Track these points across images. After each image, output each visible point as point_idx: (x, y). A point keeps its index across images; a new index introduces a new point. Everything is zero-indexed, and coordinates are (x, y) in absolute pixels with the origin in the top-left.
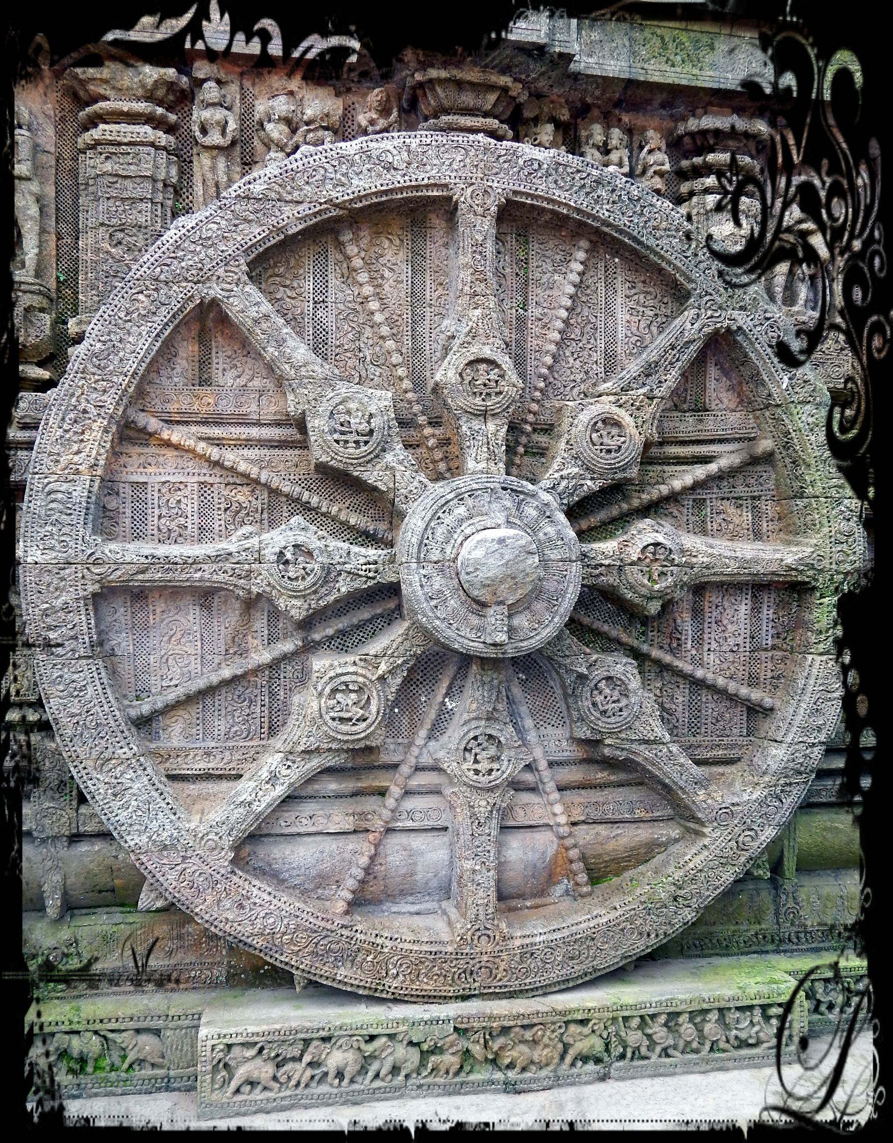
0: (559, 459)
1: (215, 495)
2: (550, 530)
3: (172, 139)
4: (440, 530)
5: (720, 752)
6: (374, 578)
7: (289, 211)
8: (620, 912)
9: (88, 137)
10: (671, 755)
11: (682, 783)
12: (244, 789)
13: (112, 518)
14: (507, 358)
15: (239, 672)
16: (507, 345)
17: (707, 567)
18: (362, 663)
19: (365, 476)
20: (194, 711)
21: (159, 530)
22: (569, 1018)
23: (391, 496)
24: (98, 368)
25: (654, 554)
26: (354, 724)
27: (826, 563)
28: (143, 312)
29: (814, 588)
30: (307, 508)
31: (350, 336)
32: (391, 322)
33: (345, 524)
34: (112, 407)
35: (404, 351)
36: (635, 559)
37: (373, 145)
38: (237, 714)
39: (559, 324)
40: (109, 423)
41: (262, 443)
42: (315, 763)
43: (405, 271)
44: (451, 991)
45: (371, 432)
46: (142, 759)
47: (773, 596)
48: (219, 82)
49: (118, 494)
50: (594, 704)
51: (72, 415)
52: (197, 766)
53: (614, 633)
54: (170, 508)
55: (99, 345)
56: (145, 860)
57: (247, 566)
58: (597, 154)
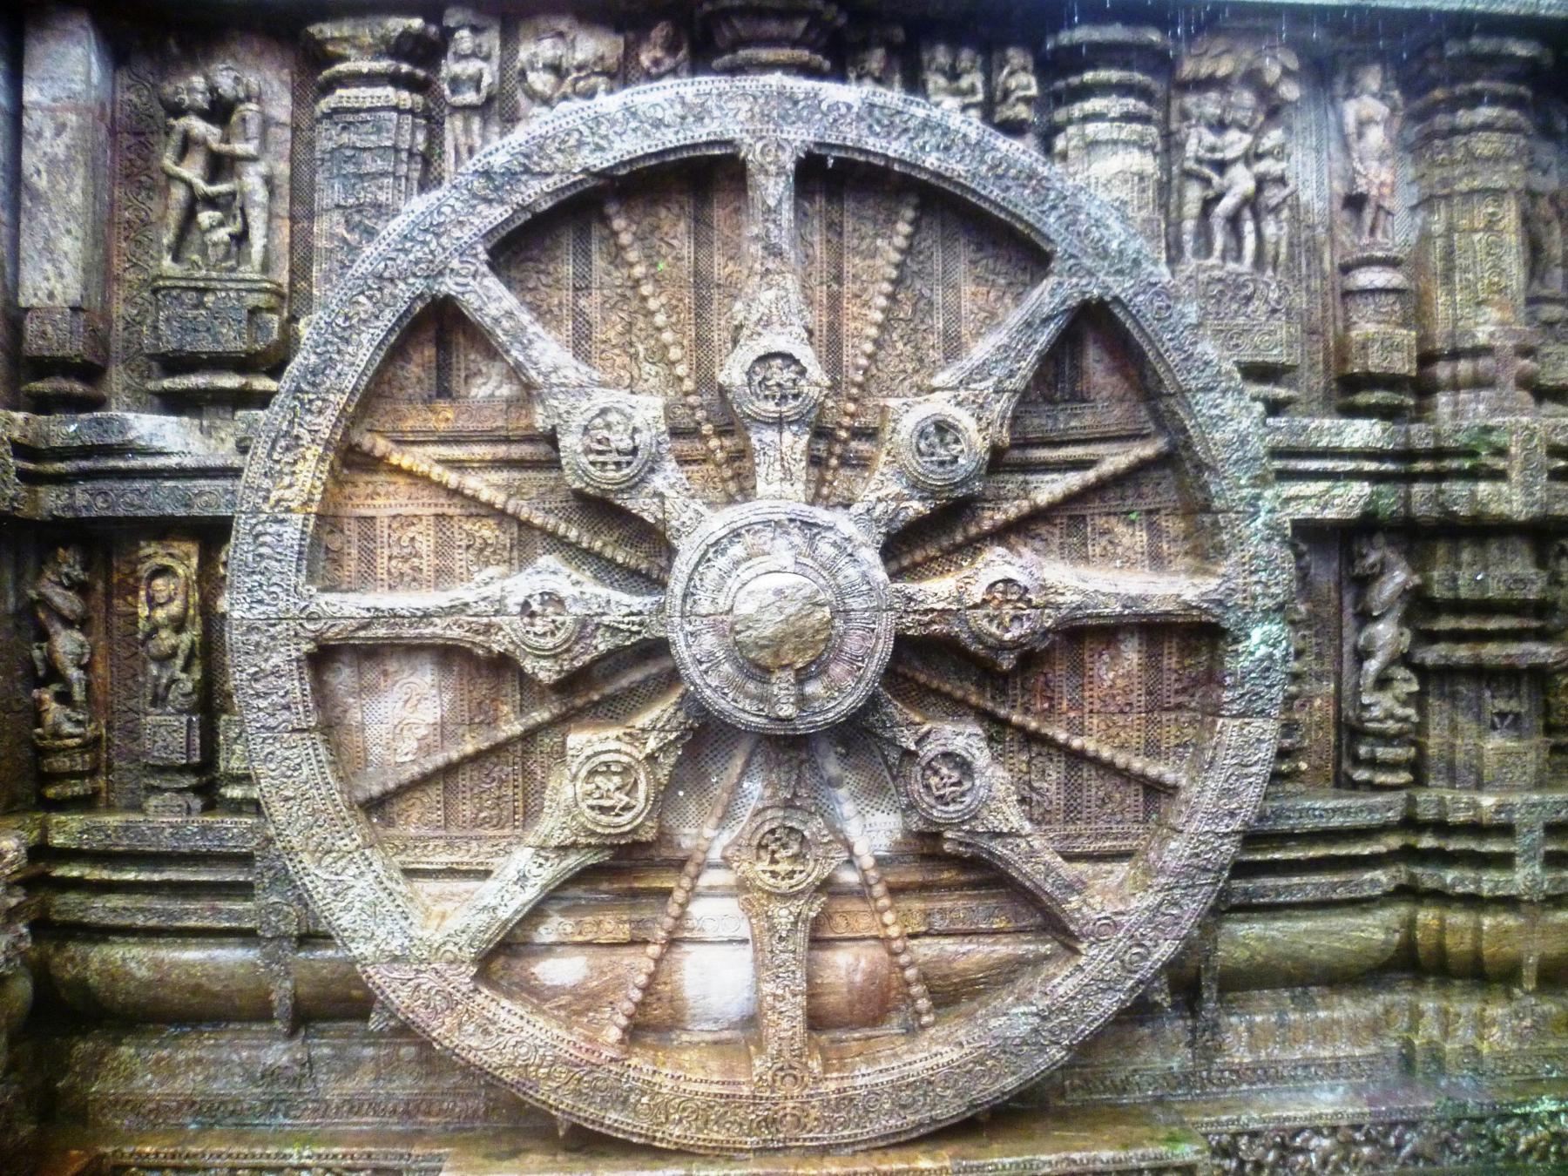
0: (877, 475)
2: (852, 572)
3: (419, 98)
5: (1108, 844)
6: (639, 633)
8: (967, 1049)
9: (325, 104)
10: (1032, 853)
12: (486, 891)
13: (335, 561)
14: (809, 351)
15: (485, 745)
16: (811, 333)
17: (1079, 608)
18: (627, 739)
19: (630, 505)
20: (435, 793)
21: (389, 572)
25: (1004, 593)
26: (617, 815)
28: (363, 316)
32: (671, 309)
33: (612, 561)
34: (328, 431)
35: (686, 342)
36: (978, 600)
37: (638, 99)
38: (485, 796)
39: (882, 302)
40: (326, 449)
42: (573, 861)
46: (368, 852)
49: (342, 531)
50: (927, 787)
51: (283, 443)
57: (485, 620)
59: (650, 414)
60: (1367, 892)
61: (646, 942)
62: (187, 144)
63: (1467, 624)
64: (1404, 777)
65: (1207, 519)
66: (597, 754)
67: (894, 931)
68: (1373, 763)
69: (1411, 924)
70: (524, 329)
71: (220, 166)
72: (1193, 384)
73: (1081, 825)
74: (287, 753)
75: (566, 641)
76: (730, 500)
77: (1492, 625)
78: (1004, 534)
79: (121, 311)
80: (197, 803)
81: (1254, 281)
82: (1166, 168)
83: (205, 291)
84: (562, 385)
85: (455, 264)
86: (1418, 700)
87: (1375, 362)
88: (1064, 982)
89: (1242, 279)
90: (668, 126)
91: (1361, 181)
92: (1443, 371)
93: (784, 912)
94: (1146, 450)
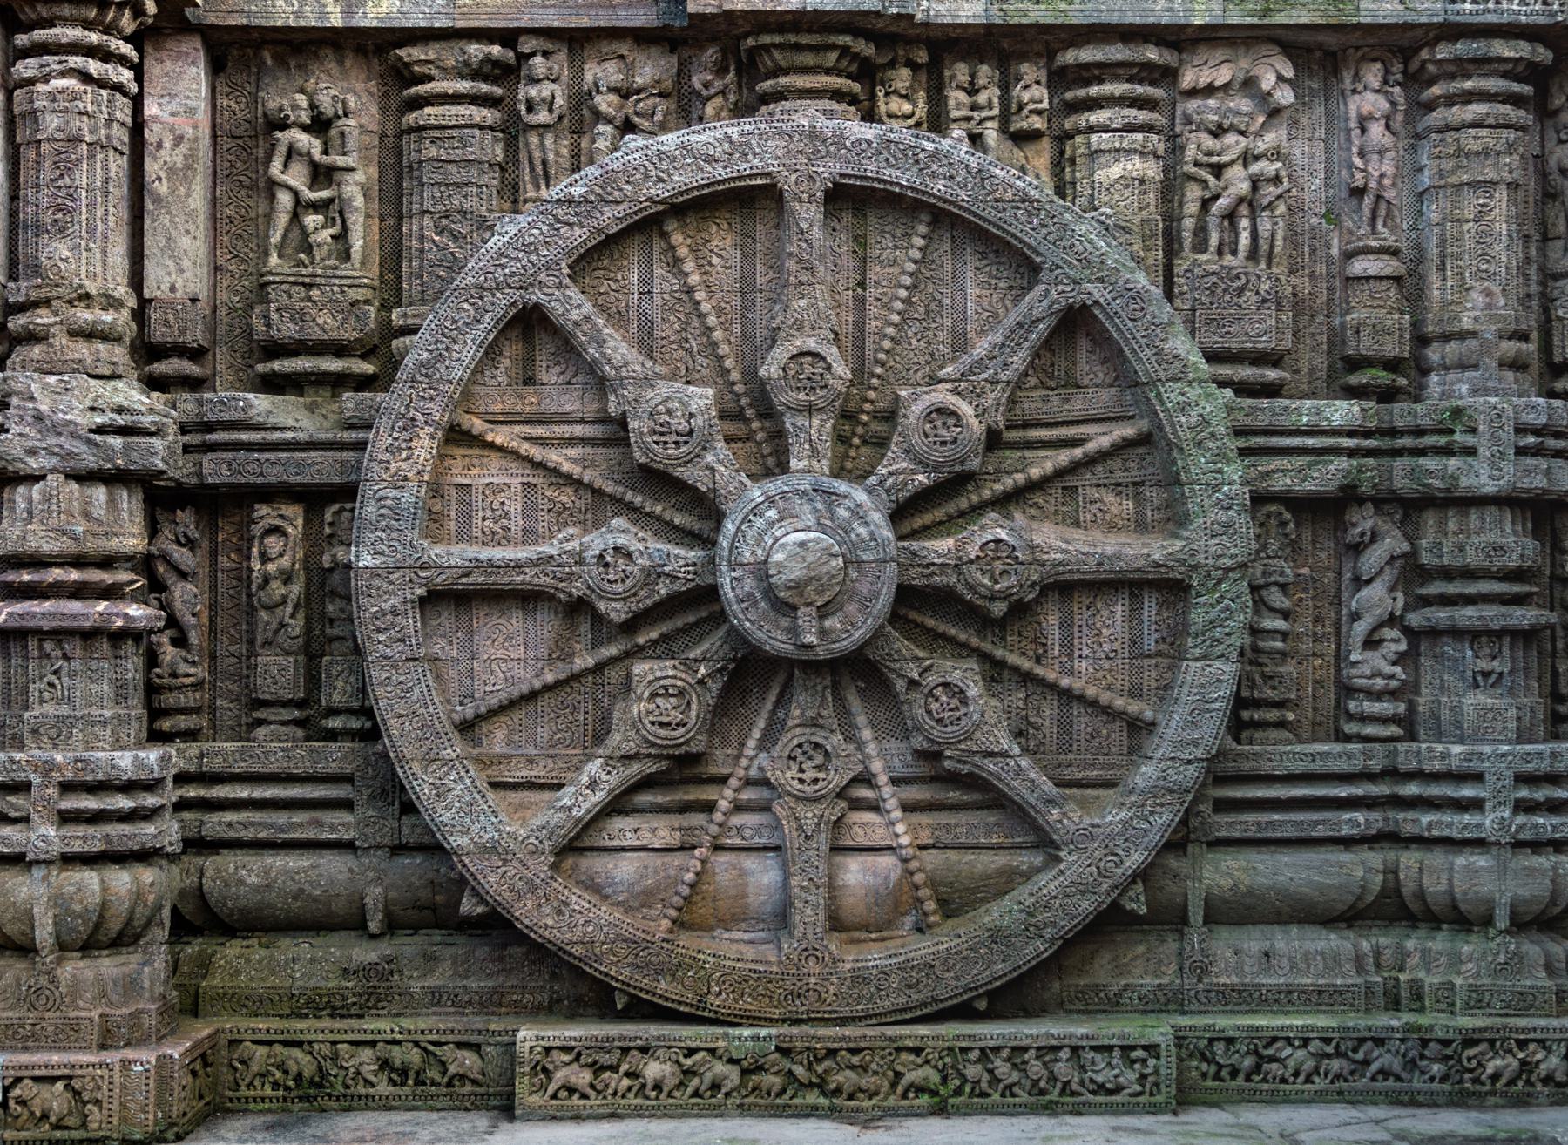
4: (750, 533)
7: (609, 212)
10: (1019, 771)
11: (1032, 801)
14: (834, 350)
15: (562, 676)
16: (836, 334)
17: (1061, 564)
19: (685, 476)
22: (900, 1044)
24: (426, 376)
25: (996, 551)
27: (1201, 558)
30: (629, 509)
31: (676, 326)
32: (720, 312)
33: (669, 524)
36: (972, 556)
37: (694, 138)
41: (584, 441)
42: (636, 768)
43: (735, 256)
44: (777, 1013)
45: (691, 432)
48: (546, 54)
50: (929, 712)
52: (518, 774)
53: (962, 637)
55: (426, 355)
58: (962, 96)
59: (702, 403)
60: (1346, 831)
61: (694, 847)
62: (291, 153)
67: (905, 840)
68: (1363, 719)
70: (599, 331)
71: (321, 174)
72: (1162, 374)
73: (1071, 756)
74: (402, 678)
76: (768, 474)
78: (1005, 502)
79: (225, 298)
80: (300, 733)
81: (1246, 274)
83: (311, 286)
85: (543, 277)
87: (1366, 345)
88: (1048, 883)
92: (1433, 354)
94: (1128, 431)
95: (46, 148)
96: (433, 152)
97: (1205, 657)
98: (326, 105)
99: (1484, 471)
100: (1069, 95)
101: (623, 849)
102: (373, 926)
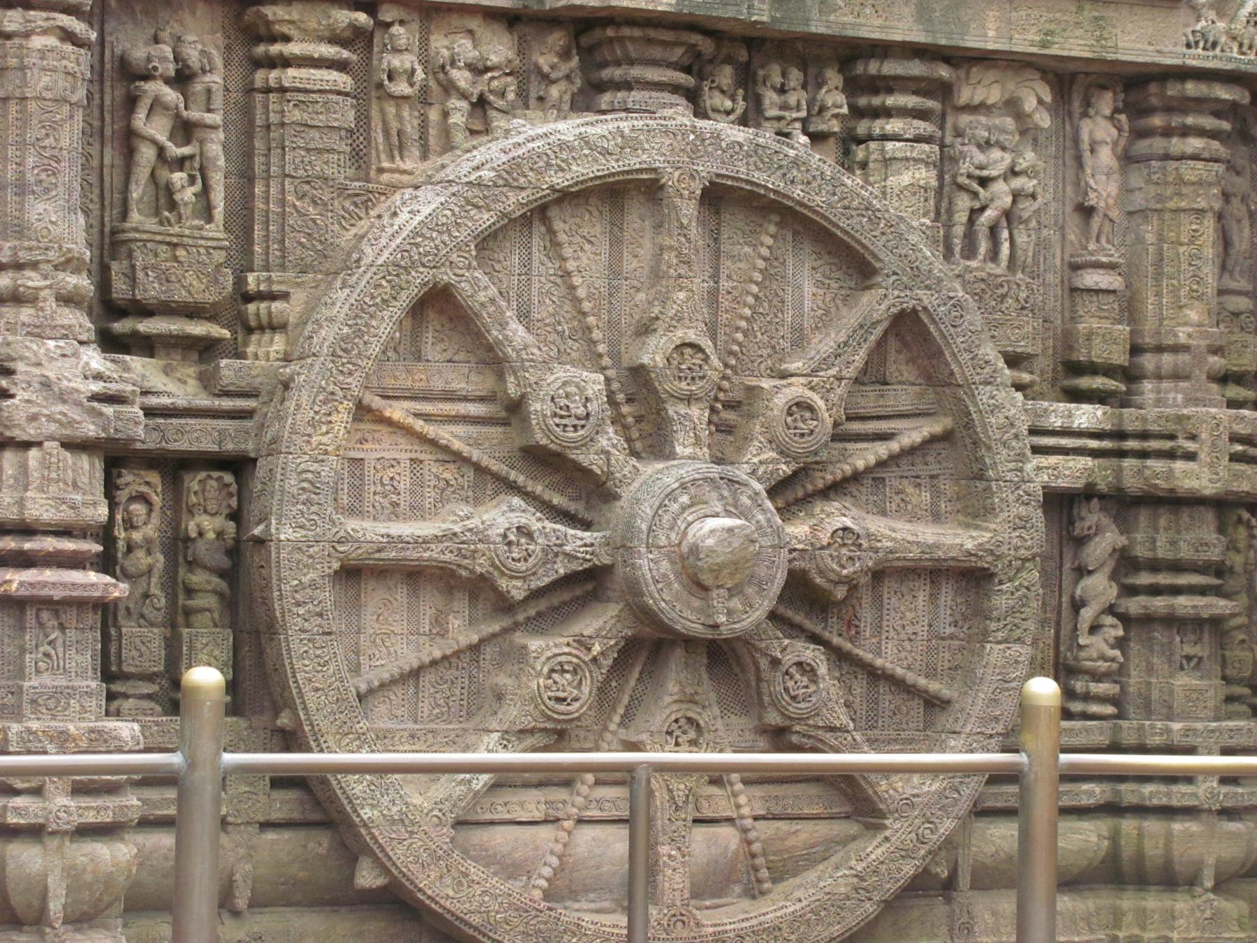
1: (426, 472)
6: (589, 560)
17: (891, 552)
18: (575, 645)
19: (581, 458)
20: (398, 692)
23: (604, 479)
25: (842, 538)
29: (992, 575)
31: (551, 309)
37: (590, 130)
43: (605, 248)
47: (951, 582)
50: (787, 690)
54: (383, 484)
55: (346, 330)
56: (377, 834)
58: (774, 96)
60: (1085, 801)
61: (557, 820)
62: (157, 104)
63: (1164, 579)
64: (1109, 710)
65: (980, 485)
66: (556, 655)
69: (1115, 837)
71: (185, 130)
72: (977, 378)
73: (876, 732)
74: (318, 652)
75: (535, 566)
77: (1183, 580)
82: (940, 177)
83: (175, 245)
84: (532, 360)
85: (454, 257)
86: (1121, 643)
87: (1099, 352)
88: (875, 850)
89: (1000, 280)
90: (611, 154)
91: (1092, 195)
92: (1148, 362)
93: (682, 787)
95: (32, 106)
96: (296, 115)
97: (1005, 641)
98: (193, 56)
99: (1206, 474)
100: (863, 101)
101: (492, 823)
102: (241, 903)
